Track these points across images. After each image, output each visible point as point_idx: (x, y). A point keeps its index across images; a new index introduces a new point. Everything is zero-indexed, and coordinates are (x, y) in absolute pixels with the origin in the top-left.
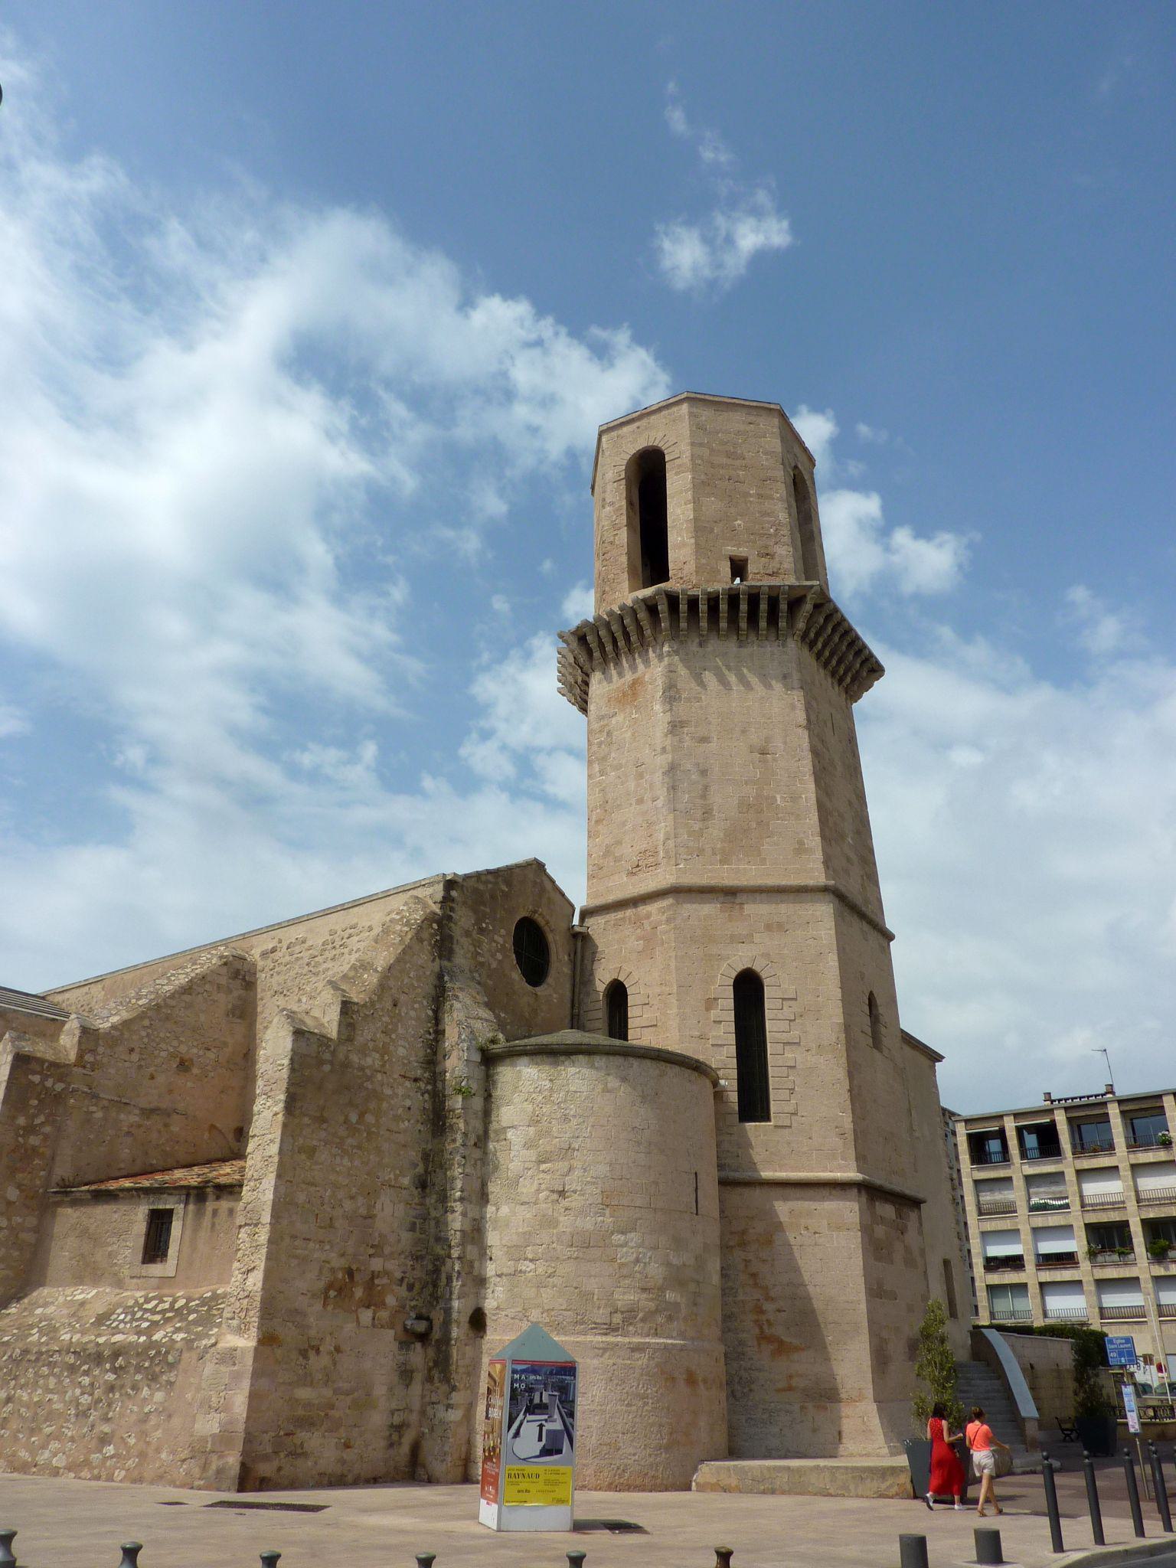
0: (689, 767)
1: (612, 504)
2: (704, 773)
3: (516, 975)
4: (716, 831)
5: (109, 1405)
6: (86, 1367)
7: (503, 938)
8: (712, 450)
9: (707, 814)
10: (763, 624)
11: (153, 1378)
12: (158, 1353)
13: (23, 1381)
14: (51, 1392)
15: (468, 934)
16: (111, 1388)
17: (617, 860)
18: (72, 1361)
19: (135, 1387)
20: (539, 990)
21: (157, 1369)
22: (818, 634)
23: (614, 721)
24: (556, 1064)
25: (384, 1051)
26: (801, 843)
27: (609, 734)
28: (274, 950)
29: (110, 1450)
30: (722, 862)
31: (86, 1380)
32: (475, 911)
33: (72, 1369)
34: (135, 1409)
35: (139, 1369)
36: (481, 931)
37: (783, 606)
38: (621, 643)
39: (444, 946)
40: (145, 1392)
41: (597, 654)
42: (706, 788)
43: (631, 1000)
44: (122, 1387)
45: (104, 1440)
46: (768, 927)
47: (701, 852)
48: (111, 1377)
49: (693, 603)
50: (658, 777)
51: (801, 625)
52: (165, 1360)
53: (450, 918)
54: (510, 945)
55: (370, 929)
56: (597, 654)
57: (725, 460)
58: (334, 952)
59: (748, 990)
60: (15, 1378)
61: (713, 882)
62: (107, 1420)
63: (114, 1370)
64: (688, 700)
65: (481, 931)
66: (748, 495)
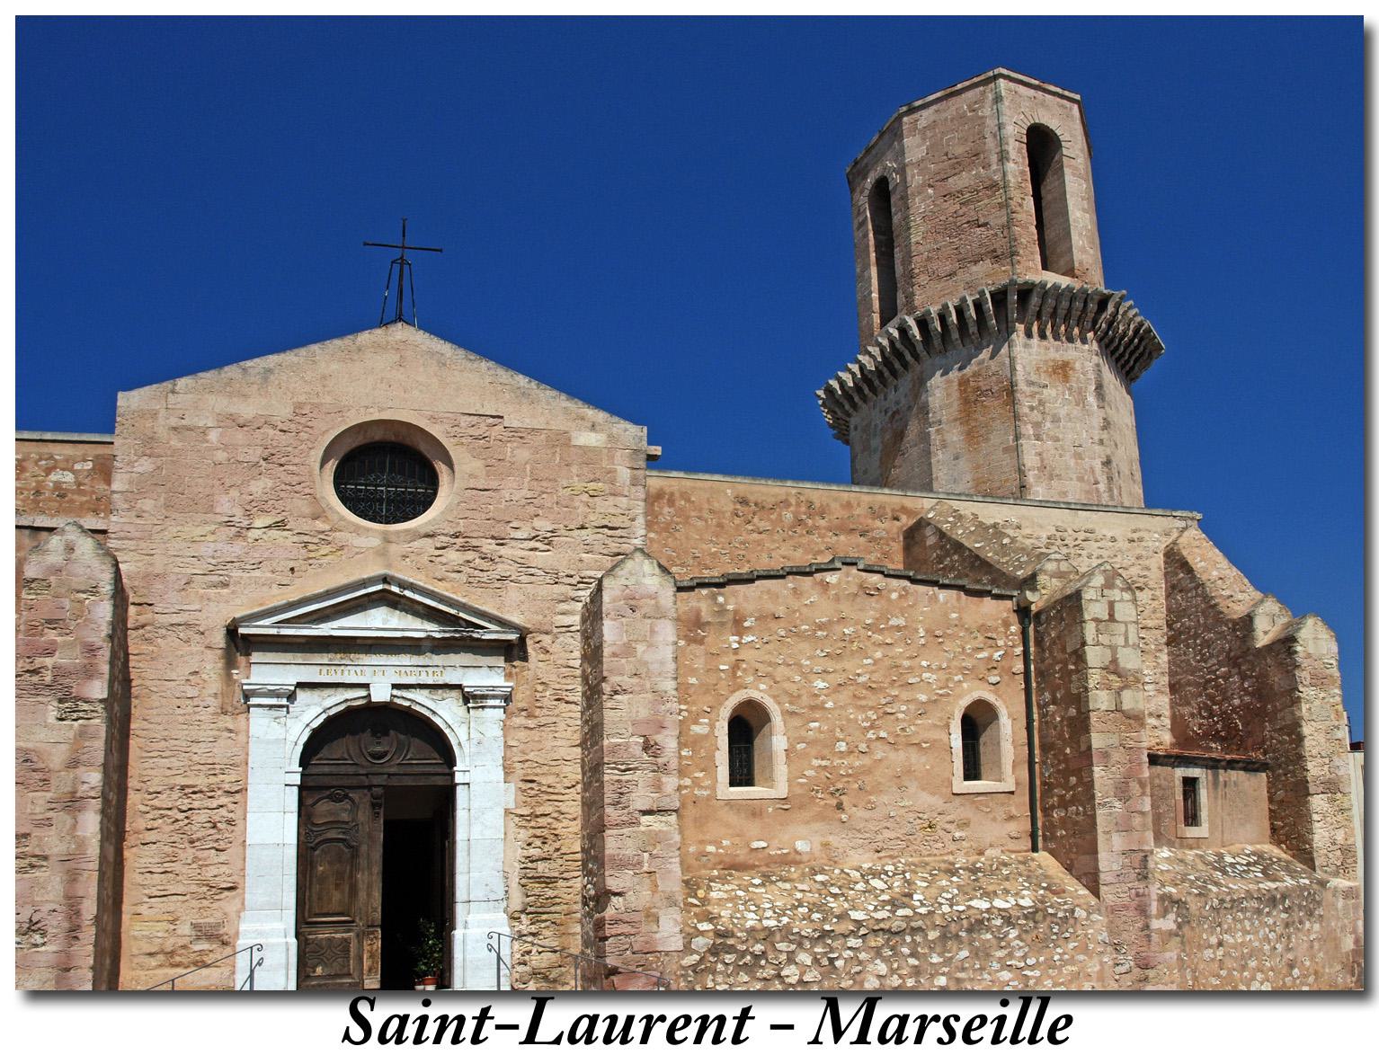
5: (1289, 938)
6: (1267, 910)
11: (1310, 914)
12: (1309, 893)
13: (1226, 926)
14: (1249, 933)
16: (1287, 925)
18: (1256, 905)
19: (1301, 922)
21: (1311, 906)
29: (1296, 972)
31: (1271, 921)
33: (1259, 912)
34: (1305, 938)
35: (1300, 907)
40: (1308, 925)
44: (1294, 922)
45: (1291, 966)
48: (1284, 916)
52: (1314, 900)
55: (1113, 540)
58: (1064, 551)
60: (1220, 925)
62: (1289, 949)
63: (1286, 910)
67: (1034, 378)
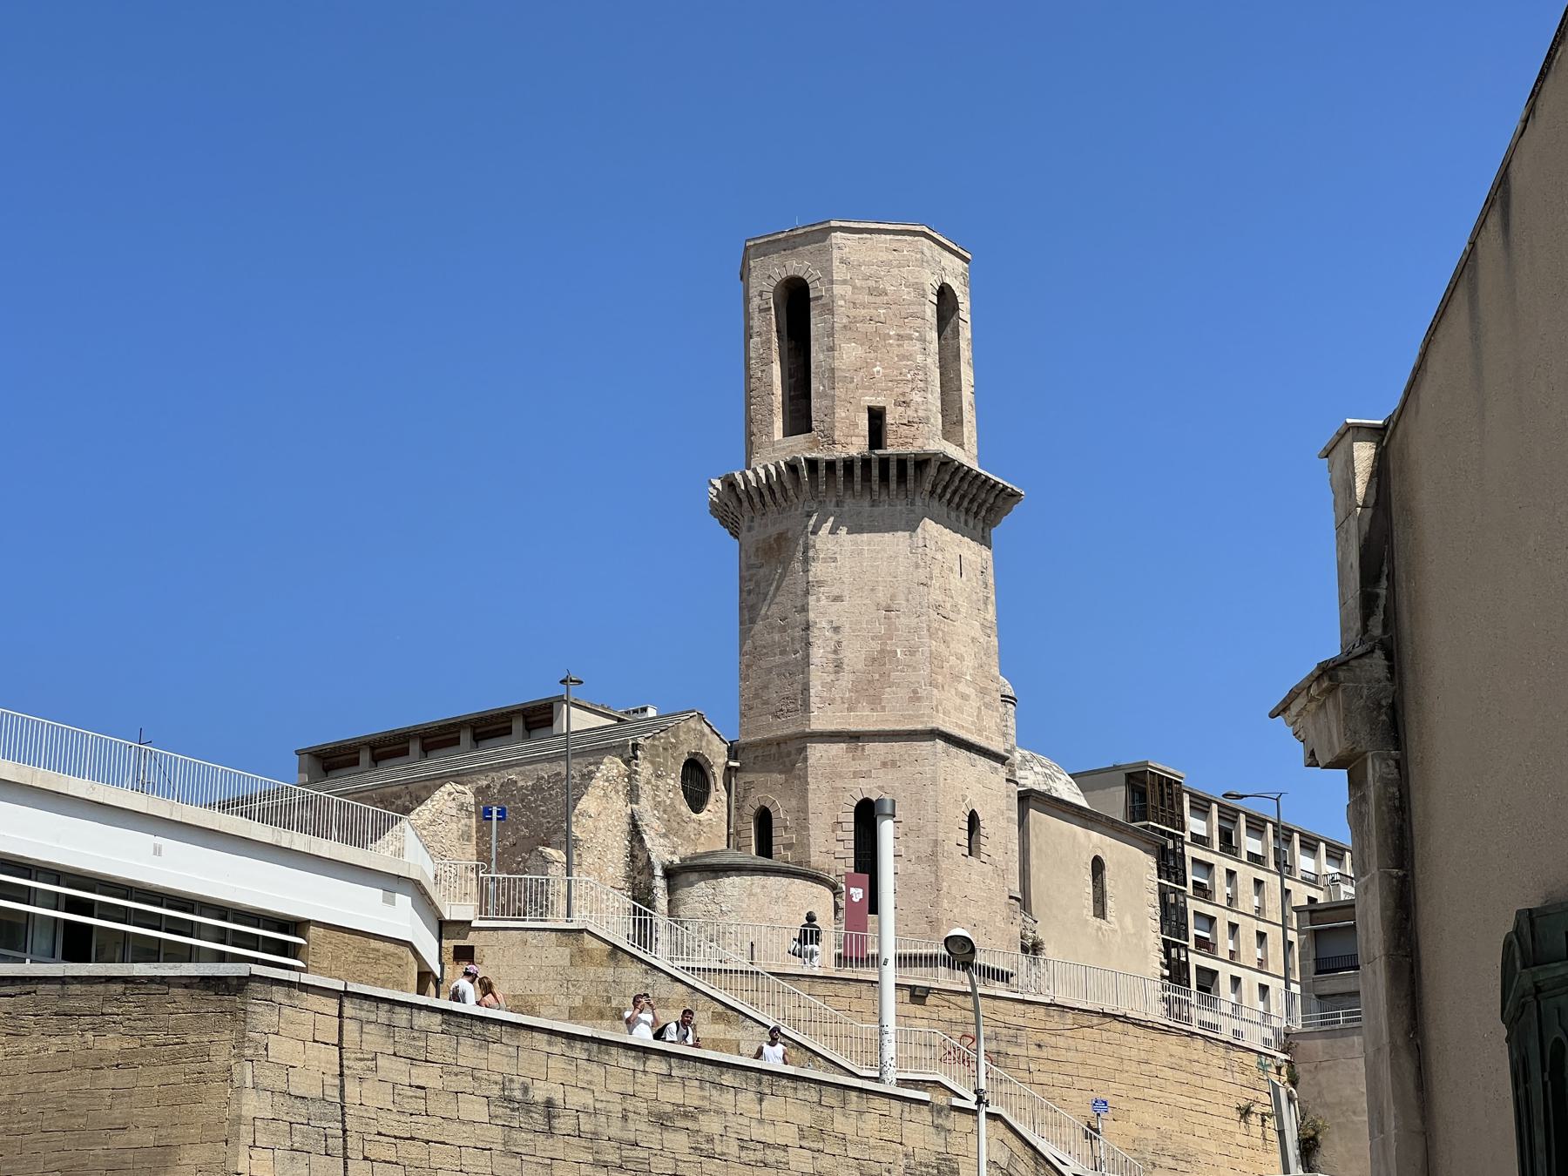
0: (824, 624)
1: (760, 335)
2: (836, 629)
3: (684, 808)
4: (846, 679)
7: (674, 780)
8: (854, 287)
9: (838, 667)
10: (893, 485)
15: (648, 782)
17: (766, 703)
20: (703, 816)
22: (945, 488)
23: (762, 571)
24: (716, 878)
25: (600, 871)
26: (915, 692)
27: (758, 584)
28: (488, 787)
30: (850, 709)
32: (652, 763)
36: (658, 776)
37: (911, 471)
38: (768, 498)
39: (633, 795)
41: (746, 504)
42: (839, 643)
43: (775, 823)
46: (884, 764)
47: (831, 702)
49: (831, 465)
50: (798, 633)
51: (928, 487)
53: (636, 772)
54: (679, 784)
56: (746, 504)
57: (867, 298)
59: (867, 815)
61: (839, 728)
64: (825, 560)
65: (658, 776)
66: (890, 337)
67: (753, 560)
